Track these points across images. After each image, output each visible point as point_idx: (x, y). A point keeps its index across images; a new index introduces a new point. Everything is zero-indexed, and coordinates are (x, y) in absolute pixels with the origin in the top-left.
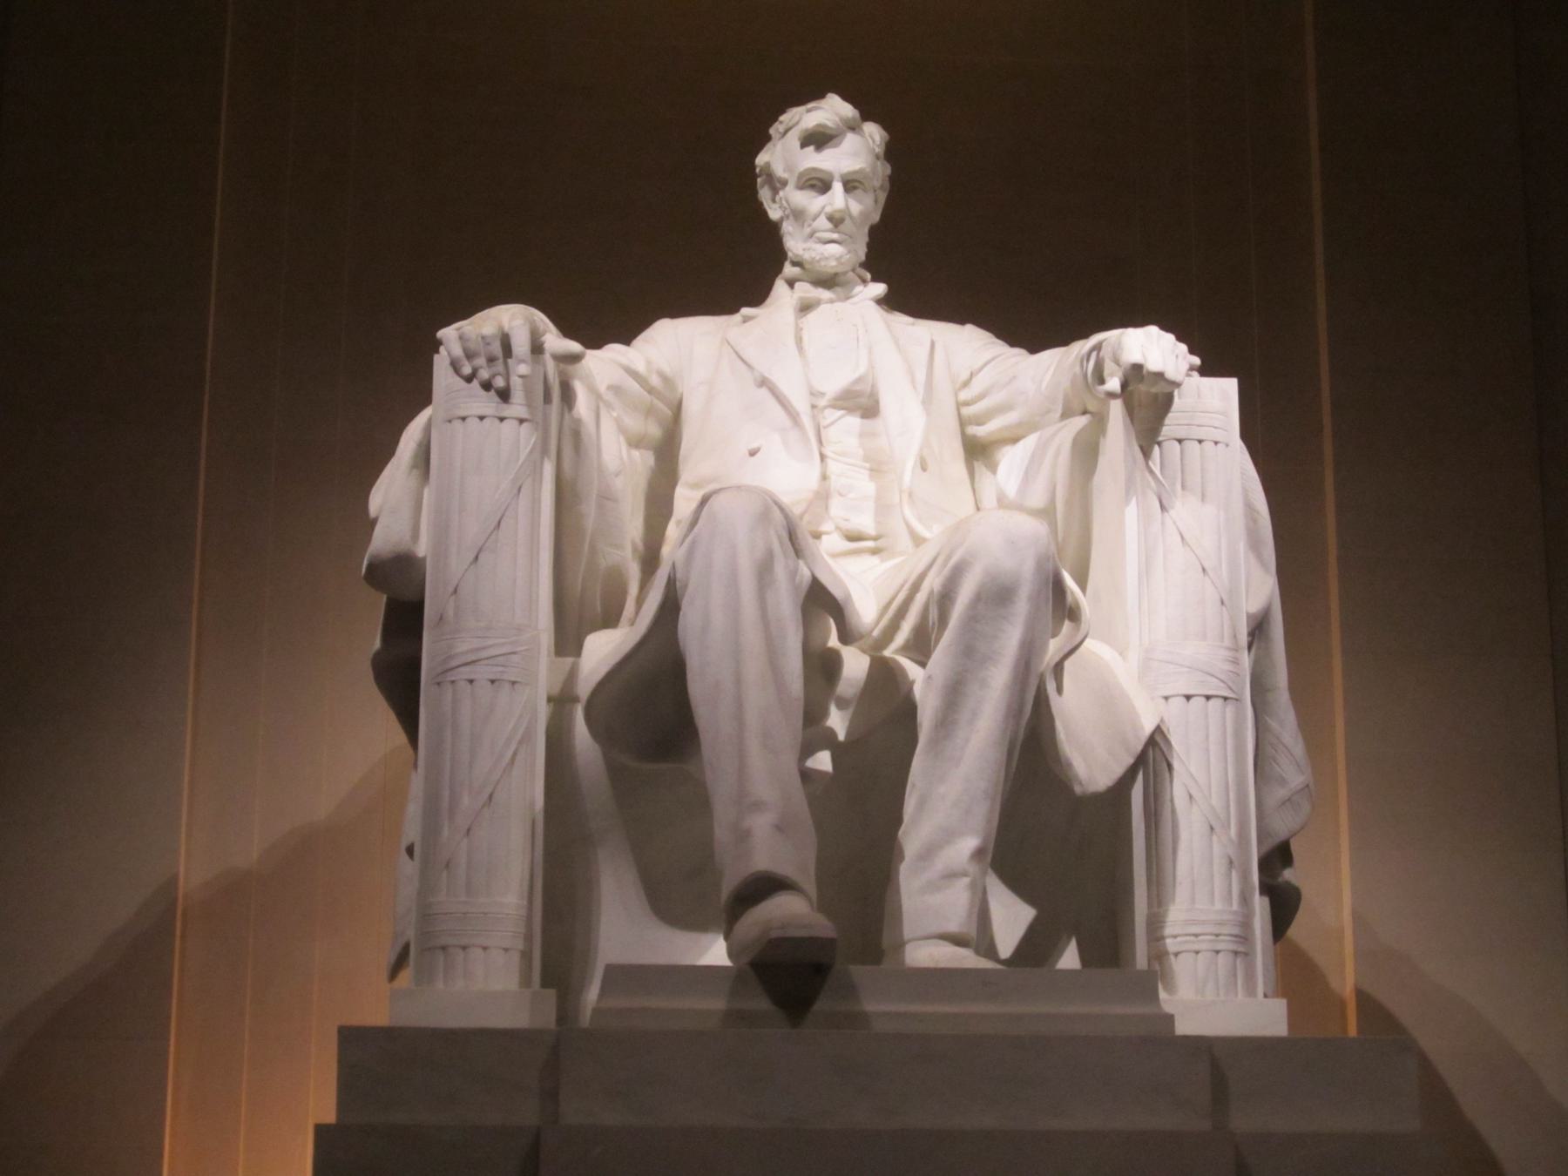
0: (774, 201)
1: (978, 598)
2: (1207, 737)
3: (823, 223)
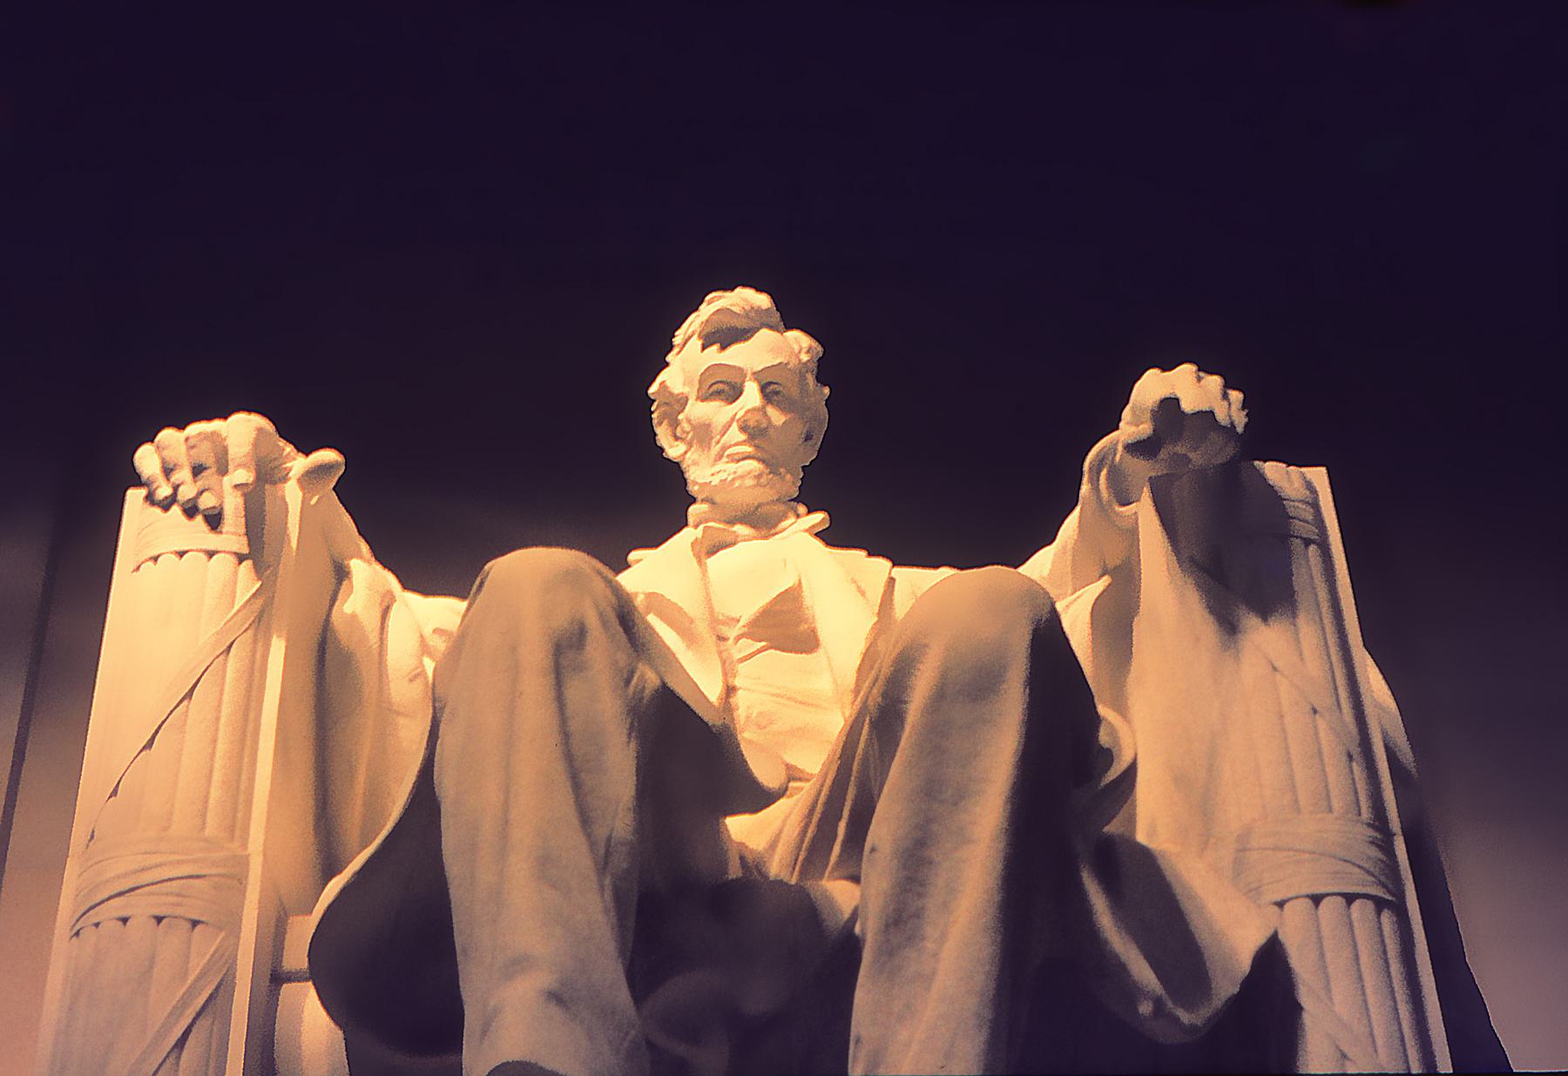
0: (677, 438)
1: (940, 696)
2: (1357, 958)
3: (735, 434)
